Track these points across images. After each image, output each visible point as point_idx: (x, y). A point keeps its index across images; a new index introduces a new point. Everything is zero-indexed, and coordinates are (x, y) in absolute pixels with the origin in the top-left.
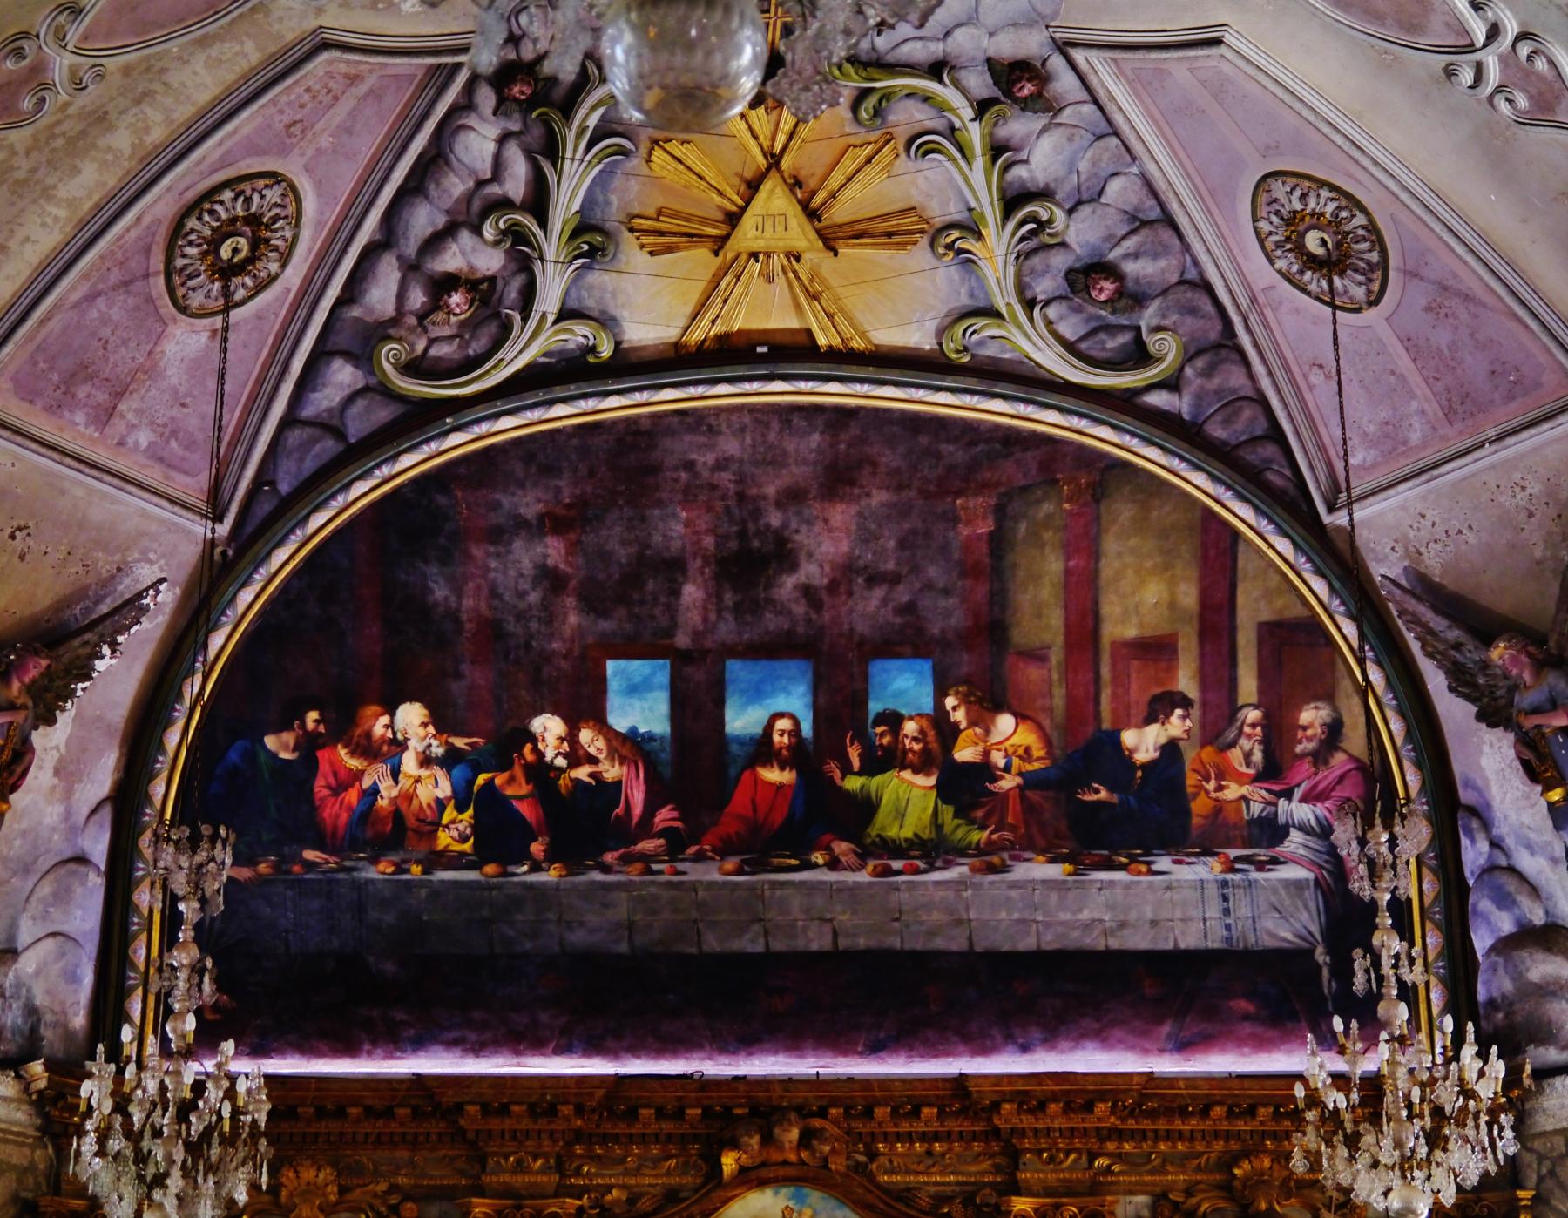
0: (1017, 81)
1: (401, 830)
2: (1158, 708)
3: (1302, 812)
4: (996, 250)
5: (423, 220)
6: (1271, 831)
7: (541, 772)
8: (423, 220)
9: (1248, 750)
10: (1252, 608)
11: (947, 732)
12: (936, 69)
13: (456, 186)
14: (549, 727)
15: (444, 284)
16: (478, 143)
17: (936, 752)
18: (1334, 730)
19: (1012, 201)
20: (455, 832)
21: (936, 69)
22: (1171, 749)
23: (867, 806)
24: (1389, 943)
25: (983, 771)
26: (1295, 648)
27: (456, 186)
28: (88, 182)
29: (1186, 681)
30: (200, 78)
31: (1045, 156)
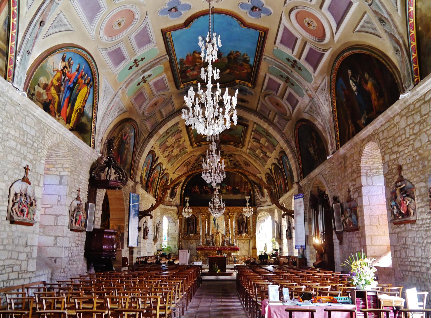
0: (230, 156)
1: (196, 193)
2: (238, 186)
3: (246, 192)
4: (229, 163)
5: (198, 161)
6: (244, 193)
7: (204, 189)
8: (198, 161)
9: (243, 188)
10: (243, 181)
11: (226, 187)
12: (226, 155)
13: (200, 160)
14: (204, 187)
15: (199, 165)
16: (201, 158)
17: (226, 189)
18: (248, 187)
19: (230, 161)
20: (199, 193)
21: (226, 155)
22: (239, 188)
23: (222, 191)
24: (248, 203)
25: (228, 189)
26: (246, 183)
27: (200, 160)
28: (181, 162)
29: (240, 184)
30: (187, 158)
31: (232, 159)
